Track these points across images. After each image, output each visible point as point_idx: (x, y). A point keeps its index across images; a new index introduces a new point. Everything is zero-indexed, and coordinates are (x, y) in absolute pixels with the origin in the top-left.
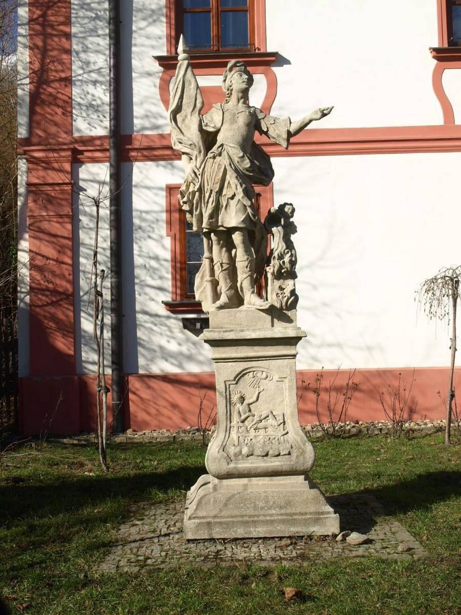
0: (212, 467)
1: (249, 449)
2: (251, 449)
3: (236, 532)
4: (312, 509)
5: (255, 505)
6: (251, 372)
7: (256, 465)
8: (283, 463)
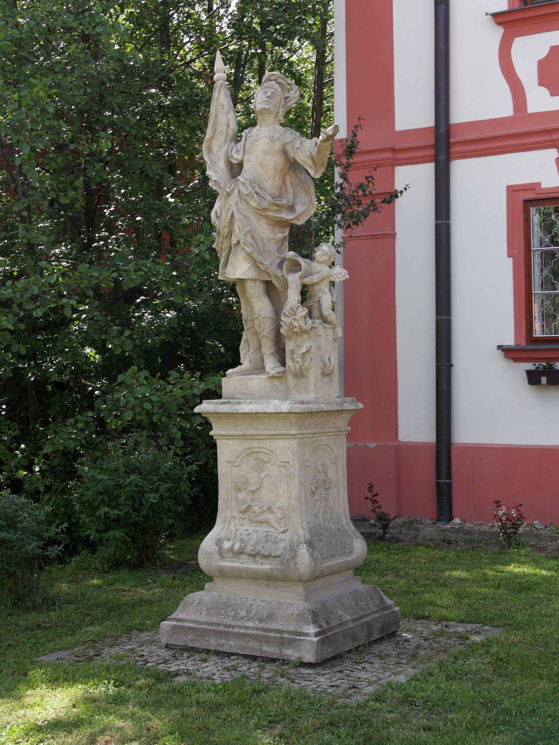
0: (203, 563)
1: (240, 546)
2: (243, 546)
3: (208, 642)
4: (291, 628)
5: (235, 614)
6: (254, 452)
7: (248, 566)
8: (273, 567)
